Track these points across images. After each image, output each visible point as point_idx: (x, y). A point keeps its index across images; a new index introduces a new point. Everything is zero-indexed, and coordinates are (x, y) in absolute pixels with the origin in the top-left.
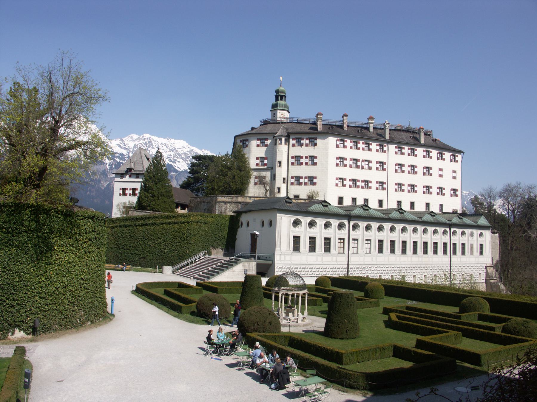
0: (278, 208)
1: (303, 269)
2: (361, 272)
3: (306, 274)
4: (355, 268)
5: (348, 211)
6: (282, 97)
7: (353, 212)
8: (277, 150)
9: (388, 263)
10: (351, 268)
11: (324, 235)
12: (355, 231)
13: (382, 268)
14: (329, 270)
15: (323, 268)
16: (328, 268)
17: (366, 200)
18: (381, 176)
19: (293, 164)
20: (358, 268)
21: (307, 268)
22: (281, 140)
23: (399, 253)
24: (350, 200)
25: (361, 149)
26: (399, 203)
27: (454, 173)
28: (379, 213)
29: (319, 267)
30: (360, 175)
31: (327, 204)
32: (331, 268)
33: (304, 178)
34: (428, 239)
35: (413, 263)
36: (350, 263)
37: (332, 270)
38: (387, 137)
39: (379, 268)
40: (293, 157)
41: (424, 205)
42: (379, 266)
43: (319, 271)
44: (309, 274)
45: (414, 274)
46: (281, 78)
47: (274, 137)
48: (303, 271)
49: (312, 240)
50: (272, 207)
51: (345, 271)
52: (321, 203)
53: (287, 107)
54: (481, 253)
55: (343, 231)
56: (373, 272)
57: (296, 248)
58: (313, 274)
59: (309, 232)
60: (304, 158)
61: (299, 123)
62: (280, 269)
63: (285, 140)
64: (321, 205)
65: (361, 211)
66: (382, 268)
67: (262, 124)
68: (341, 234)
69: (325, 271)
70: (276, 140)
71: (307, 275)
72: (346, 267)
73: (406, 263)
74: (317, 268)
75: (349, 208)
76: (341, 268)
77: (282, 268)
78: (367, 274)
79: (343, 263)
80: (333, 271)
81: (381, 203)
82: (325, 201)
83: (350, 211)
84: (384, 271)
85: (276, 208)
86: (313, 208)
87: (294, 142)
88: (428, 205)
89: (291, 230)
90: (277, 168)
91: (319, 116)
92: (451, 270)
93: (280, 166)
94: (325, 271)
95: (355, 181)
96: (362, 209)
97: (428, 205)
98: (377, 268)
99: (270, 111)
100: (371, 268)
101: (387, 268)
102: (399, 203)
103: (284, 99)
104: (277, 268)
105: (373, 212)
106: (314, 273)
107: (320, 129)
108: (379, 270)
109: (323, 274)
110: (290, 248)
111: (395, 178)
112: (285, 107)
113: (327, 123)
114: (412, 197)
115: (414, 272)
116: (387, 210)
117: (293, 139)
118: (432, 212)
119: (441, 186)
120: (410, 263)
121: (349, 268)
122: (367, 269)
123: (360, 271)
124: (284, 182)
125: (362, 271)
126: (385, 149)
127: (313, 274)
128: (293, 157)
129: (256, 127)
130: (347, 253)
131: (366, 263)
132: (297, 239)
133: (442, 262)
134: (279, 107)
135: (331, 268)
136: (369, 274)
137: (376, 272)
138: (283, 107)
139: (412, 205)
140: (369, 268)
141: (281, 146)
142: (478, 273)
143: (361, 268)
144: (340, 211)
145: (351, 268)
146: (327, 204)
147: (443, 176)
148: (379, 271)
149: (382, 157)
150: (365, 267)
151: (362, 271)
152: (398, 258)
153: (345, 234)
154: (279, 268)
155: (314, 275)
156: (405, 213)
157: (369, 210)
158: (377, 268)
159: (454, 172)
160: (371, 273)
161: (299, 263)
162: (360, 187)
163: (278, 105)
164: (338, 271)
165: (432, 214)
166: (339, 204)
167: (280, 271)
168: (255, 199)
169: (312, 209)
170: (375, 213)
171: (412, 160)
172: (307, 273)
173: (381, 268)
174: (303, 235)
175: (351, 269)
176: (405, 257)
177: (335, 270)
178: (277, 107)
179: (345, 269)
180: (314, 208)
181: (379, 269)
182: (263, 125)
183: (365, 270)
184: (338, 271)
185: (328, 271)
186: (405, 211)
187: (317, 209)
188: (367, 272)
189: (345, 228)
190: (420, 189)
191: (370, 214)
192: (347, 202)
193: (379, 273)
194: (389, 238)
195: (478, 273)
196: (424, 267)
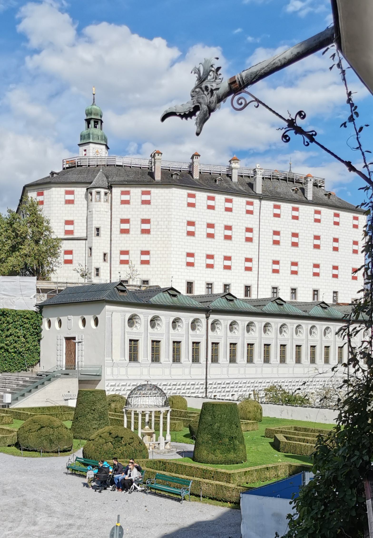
2: (223, 389)
4: (215, 384)
5: (205, 303)
6: (96, 122)
7: (213, 304)
8: (94, 210)
9: (261, 376)
10: (210, 384)
11: (173, 338)
12: (215, 332)
13: (254, 383)
14: (179, 387)
16: (178, 384)
20: (220, 384)
23: (277, 363)
24: (204, 286)
26: (275, 289)
28: (249, 305)
29: (166, 383)
31: (176, 293)
32: (183, 385)
34: (317, 341)
35: (296, 376)
36: (208, 377)
38: (259, 189)
39: (249, 383)
41: (311, 293)
42: (248, 380)
43: (167, 389)
49: (156, 343)
50: (96, 298)
51: (202, 389)
52: (166, 291)
55: (198, 331)
56: (240, 389)
59: (152, 334)
62: (112, 388)
63: (106, 194)
64: (168, 294)
66: (254, 383)
67: (67, 166)
68: (196, 336)
72: (202, 383)
73: (286, 376)
76: (196, 384)
77: (115, 385)
78: (232, 392)
80: (186, 388)
81: (247, 289)
82: (172, 289)
83: (208, 303)
88: (316, 292)
89: (126, 330)
90: (94, 238)
96: (224, 300)
97: (316, 292)
98: (245, 383)
101: (260, 383)
102: (275, 289)
104: (107, 386)
105: (240, 304)
107: (158, 177)
108: (249, 387)
109: (172, 393)
116: (258, 300)
118: (323, 303)
120: (292, 376)
121: (208, 384)
123: (223, 388)
125: (225, 388)
129: (57, 171)
130: (205, 363)
131: (230, 377)
132: (134, 343)
136: (235, 391)
139: (294, 291)
140: (236, 383)
144: (194, 303)
145: (210, 384)
146: (176, 293)
147: (339, 250)
148: (249, 388)
150: (229, 382)
151: (225, 388)
152: (275, 369)
153: (201, 336)
154: (111, 386)
156: (285, 305)
157: (235, 301)
158: (245, 383)
160: (238, 391)
164: (193, 389)
165: (324, 305)
166: (187, 292)
167: (113, 390)
168: (69, 285)
169: (155, 300)
170: (243, 306)
173: (252, 383)
175: (211, 386)
176: (285, 367)
179: (202, 386)
180: (157, 299)
181: (249, 385)
183: (230, 387)
184: (193, 389)
185: (178, 389)
187: (162, 301)
188: (232, 389)
189: (202, 327)
191: (236, 307)
193: (249, 391)
194: (262, 341)
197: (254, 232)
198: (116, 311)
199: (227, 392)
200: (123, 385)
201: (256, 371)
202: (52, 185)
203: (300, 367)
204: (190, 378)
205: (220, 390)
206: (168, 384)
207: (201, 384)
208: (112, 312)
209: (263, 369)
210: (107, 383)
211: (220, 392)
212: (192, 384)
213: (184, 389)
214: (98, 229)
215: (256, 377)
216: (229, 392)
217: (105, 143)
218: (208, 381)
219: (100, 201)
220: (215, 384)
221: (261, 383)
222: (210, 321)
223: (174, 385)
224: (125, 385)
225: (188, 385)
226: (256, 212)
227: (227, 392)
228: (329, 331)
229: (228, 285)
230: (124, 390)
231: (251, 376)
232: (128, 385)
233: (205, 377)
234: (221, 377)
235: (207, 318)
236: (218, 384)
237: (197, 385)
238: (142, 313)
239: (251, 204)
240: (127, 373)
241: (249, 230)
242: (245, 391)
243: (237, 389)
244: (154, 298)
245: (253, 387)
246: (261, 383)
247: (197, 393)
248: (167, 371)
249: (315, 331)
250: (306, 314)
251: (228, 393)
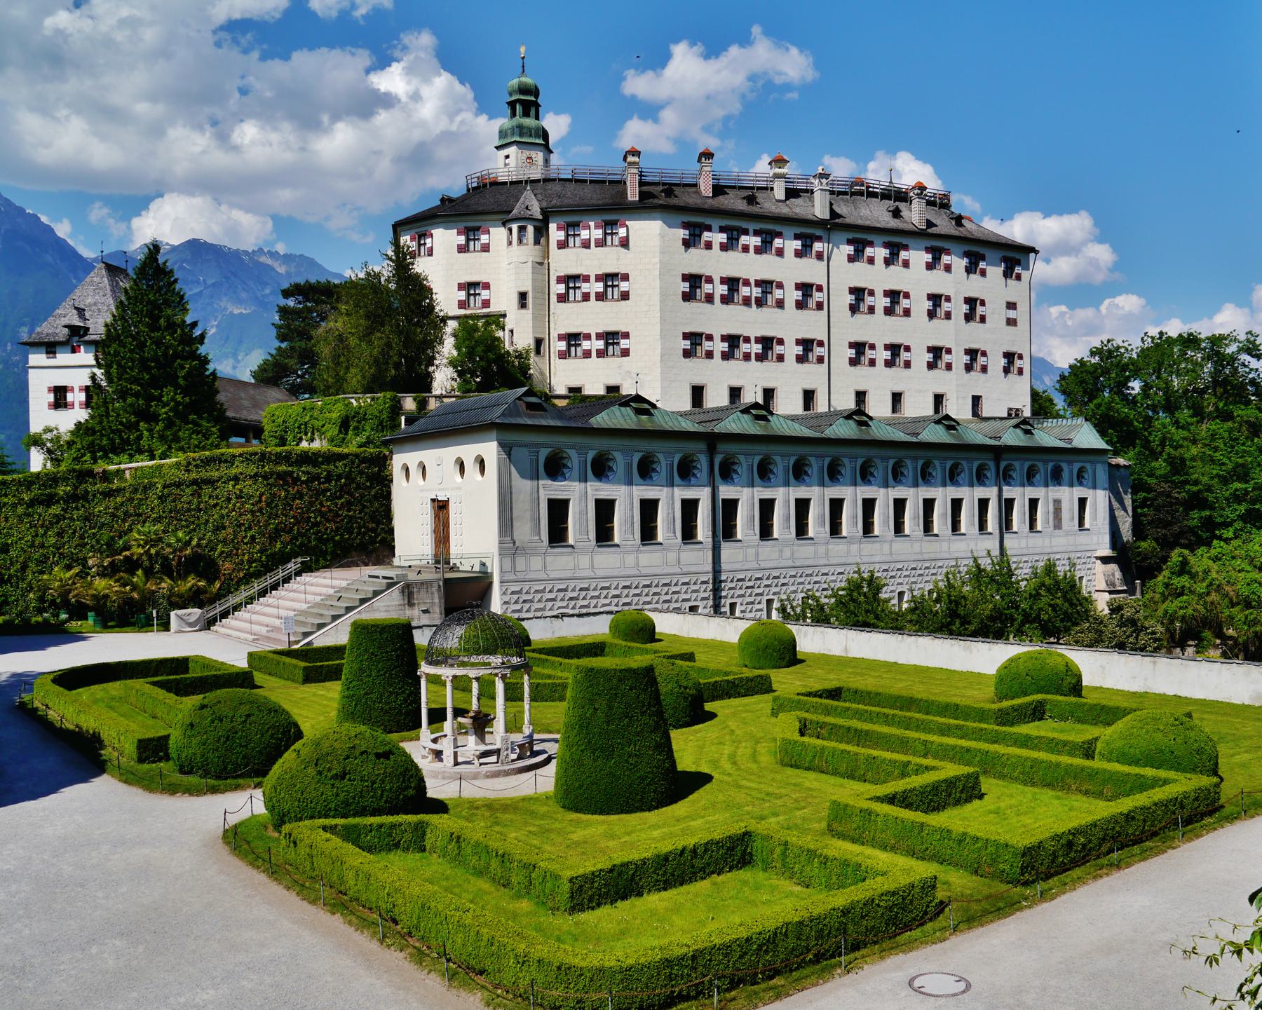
0: (497, 421)
1: (584, 593)
2: (750, 591)
3: (592, 605)
4: (732, 581)
13: (811, 575)
15: (641, 586)
17: (769, 393)
18: (810, 324)
19: (562, 298)
21: (595, 589)
22: (522, 229)
25: (752, 249)
26: (861, 396)
28: (797, 426)
30: (751, 322)
31: (646, 406)
32: (665, 585)
33: (593, 337)
37: (666, 589)
39: (801, 576)
40: (560, 280)
41: (931, 400)
43: (631, 594)
44: (600, 605)
45: (900, 589)
46: (523, 49)
47: (504, 224)
48: (584, 598)
51: (705, 591)
53: (545, 135)
56: (784, 588)
57: (558, 534)
58: (614, 604)
60: (593, 279)
61: (577, 181)
62: (515, 597)
65: (745, 425)
66: (811, 575)
69: (647, 595)
70: (510, 230)
71: (595, 607)
73: (877, 559)
74: (625, 587)
75: (711, 414)
81: (809, 396)
82: (638, 398)
83: (713, 423)
84: (817, 585)
85: (492, 423)
86: (603, 419)
87: (561, 235)
88: (939, 399)
91: (630, 159)
94: (647, 595)
95: (733, 341)
97: (939, 399)
98: (794, 576)
100: (778, 577)
101: (823, 574)
102: (861, 396)
103: (533, 112)
106: (616, 600)
108: (802, 583)
111: (849, 328)
112: (537, 136)
113: (656, 179)
114: (895, 379)
115: (898, 584)
116: (821, 416)
117: (559, 229)
119: (974, 346)
120: (889, 558)
122: (768, 582)
123: (747, 588)
124: (538, 352)
125: (752, 587)
126: (818, 246)
127: (614, 604)
128: (560, 280)
130: (710, 540)
131: (763, 565)
132: (558, 509)
133: (949, 552)
134: (521, 135)
135: (665, 585)
136: (774, 594)
137: (794, 588)
138: (531, 136)
139: (897, 398)
140: (774, 578)
143: (750, 580)
144: (684, 424)
146: (646, 406)
149: (810, 271)
151: (752, 587)
154: (513, 593)
155: (617, 605)
158: (794, 576)
161: (569, 574)
162: (753, 356)
164: (686, 592)
165: (949, 423)
170: (785, 426)
171: (894, 278)
172: (594, 602)
173: (807, 575)
174: (577, 496)
177: (677, 589)
179: (704, 586)
180: (606, 418)
182: (474, 189)
184: (686, 592)
185: (655, 594)
186: (871, 418)
188: (767, 589)
190: (920, 357)
192: (716, 398)
196: (912, 569)
198: (520, 446)
199: (757, 595)
200: (537, 592)
201: (816, 552)
202: (440, 220)
203: (904, 541)
204: (677, 570)
205: (742, 592)
207: (703, 583)
208: (511, 448)
209: (830, 547)
210: (504, 589)
211: (743, 596)
212: (684, 584)
213: (666, 594)
214: (523, 296)
215: (815, 563)
216: (761, 594)
217: (541, 141)
219: (527, 244)
220: (732, 581)
221: (827, 574)
222: (718, 459)
223: (645, 586)
224: (543, 591)
225: (676, 585)
227: (757, 595)
229: (773, 390)
230: (539, 601)
231: (807, 563)
232: (548, 590)
233: (709, 568)
234: (745, 567)
235: (711, 451)
236: (739, 580)
237: (695, 584)
238: (572, 447)
240: (545, 567)
242: (795, 592)
243: (777, 589)
244: (599, 417)
245: (809, 583)
246: (827, 574)
247: (695, 600)
248: (630, 559)
250: (914, 440)
251: (759, 598)
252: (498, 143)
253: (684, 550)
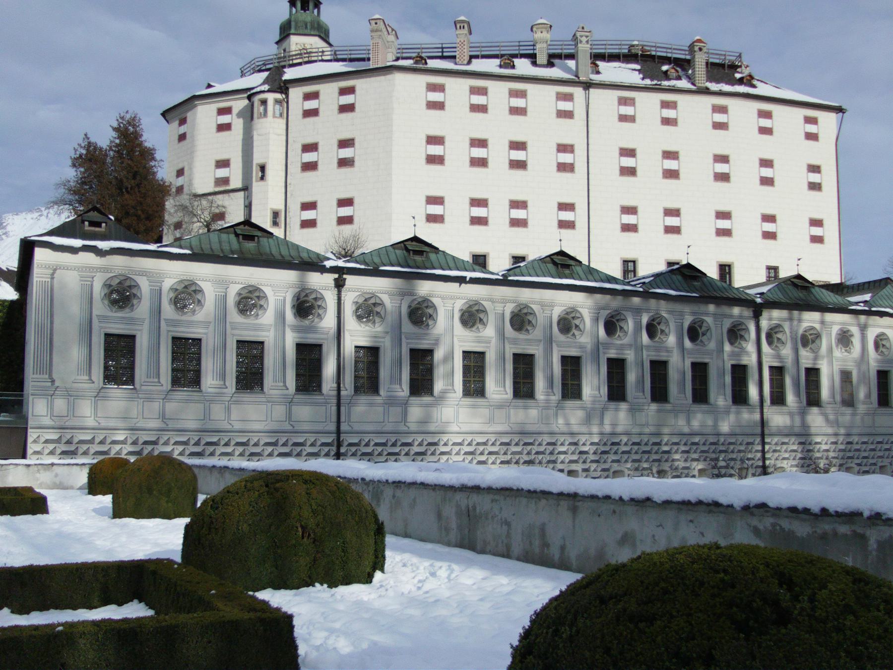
27: (814, 171)
36: (344, 427)
54: (883, 401)
72: (329, 440)
79: (319, 427)
92: (767, 456)
93: (262, 178)
99: (277, 43)
104: (35, 441)
110: (90, 375)
121: (346, 443)
130: (335, 393)
141: (264, 120)
142: (875, 464)
159: (814, 169)
163: (293, 24)
178: (290, 28)
195: (875, 464)
197: (576, 151)
206: (223, 443)
208: (55, 270)
218: (343, 436)
222: (350, 299)
226: (580, 113)
228: (704, 329)
233: (332, 427)
239: (568, 97)
241: (564, 148)
249: (663, 328)
252: (277, 38)
253: (299, 404)
